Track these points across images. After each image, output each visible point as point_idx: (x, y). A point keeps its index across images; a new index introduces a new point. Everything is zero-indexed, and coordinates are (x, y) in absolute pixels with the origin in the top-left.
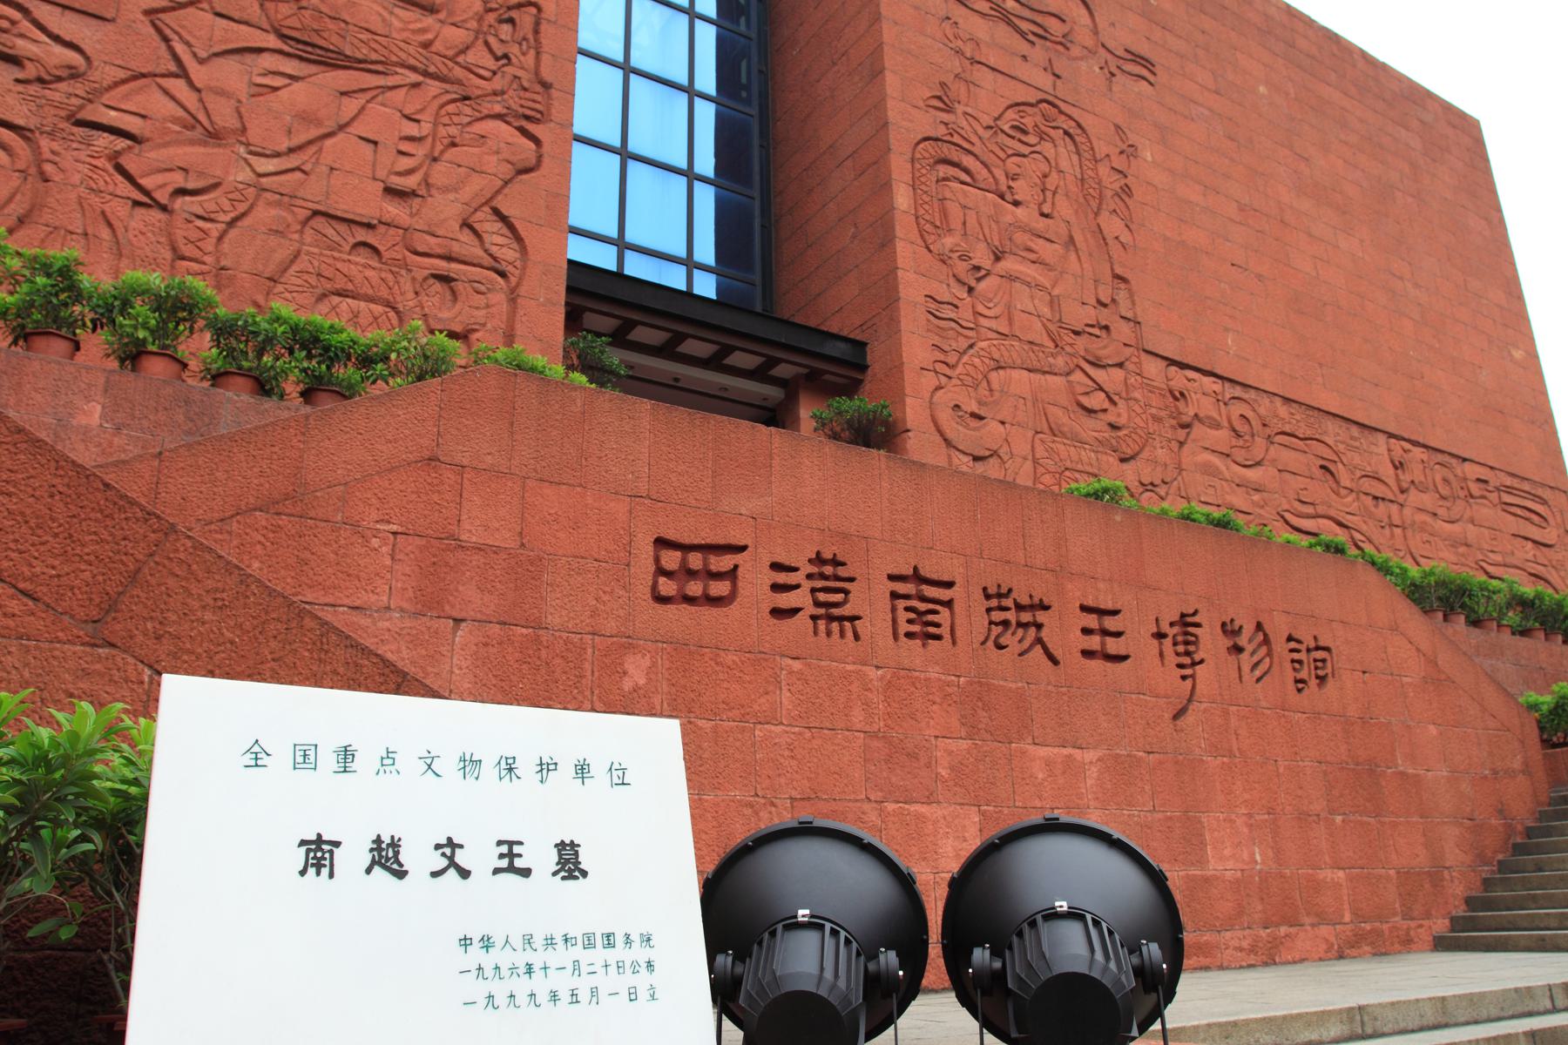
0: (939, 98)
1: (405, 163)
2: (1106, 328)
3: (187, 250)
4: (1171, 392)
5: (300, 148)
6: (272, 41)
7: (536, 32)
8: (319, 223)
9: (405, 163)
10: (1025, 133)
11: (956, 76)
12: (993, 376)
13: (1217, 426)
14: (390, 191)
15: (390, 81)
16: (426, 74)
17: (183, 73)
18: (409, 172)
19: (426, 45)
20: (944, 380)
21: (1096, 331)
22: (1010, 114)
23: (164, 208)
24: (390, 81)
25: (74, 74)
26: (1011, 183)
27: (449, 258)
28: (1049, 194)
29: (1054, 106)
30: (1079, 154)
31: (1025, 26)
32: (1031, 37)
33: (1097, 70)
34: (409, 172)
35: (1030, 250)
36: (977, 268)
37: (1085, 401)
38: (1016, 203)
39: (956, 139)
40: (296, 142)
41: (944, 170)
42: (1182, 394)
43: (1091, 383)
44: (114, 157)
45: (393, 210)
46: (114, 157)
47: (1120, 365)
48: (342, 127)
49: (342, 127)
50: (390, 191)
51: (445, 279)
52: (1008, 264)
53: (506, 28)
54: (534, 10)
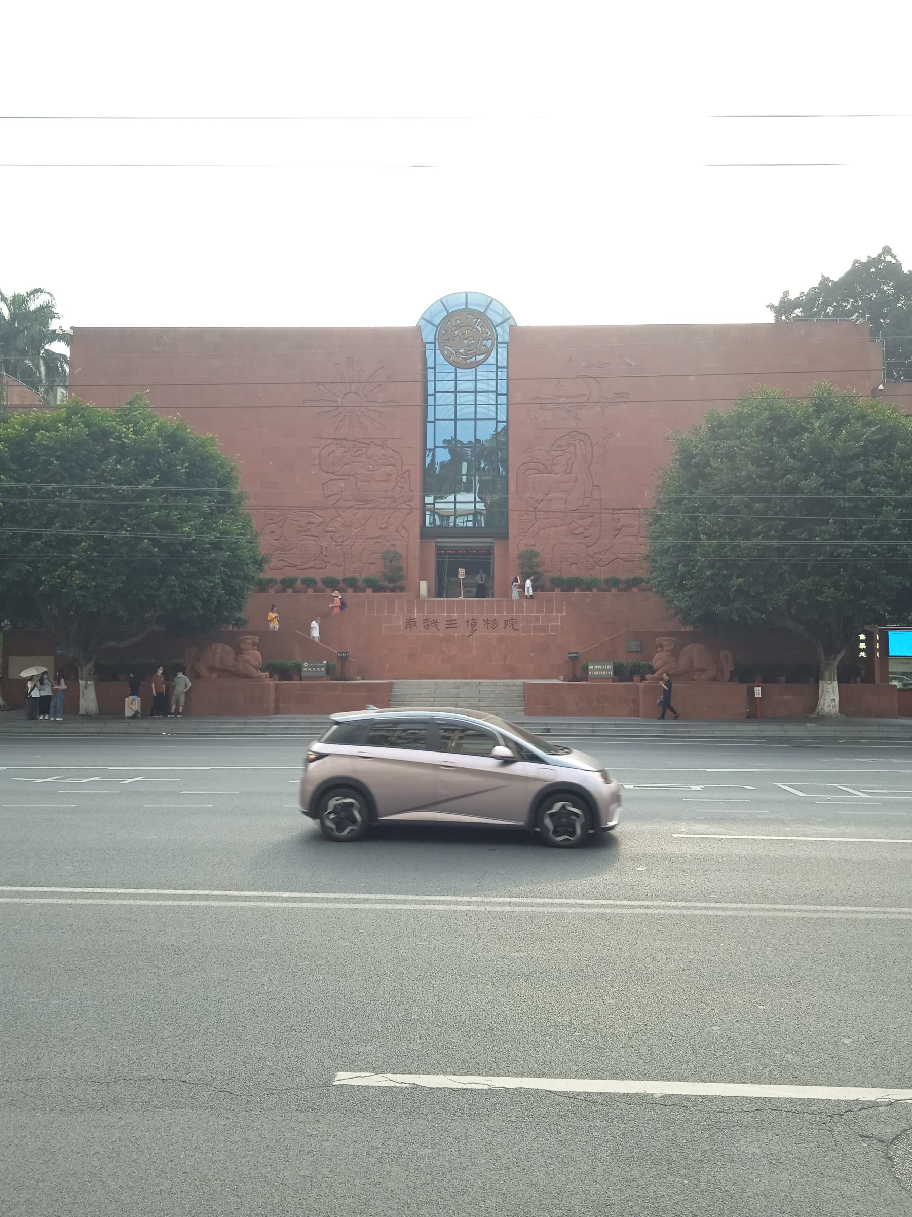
0: (529, 448)
1: (384, 521)
2: (588, 505)
3: (345, 552)
4: (614, 519)
5: (363, 525)
6: (355, 502)
7: (409, 477)
8: (368, 540)
9: (384, 521)
10: (563, 447)
11: (537, 437)
12: (541, 532)
13: (634, 526)
14: (381, 529)
15: (379, 503)
16: (385, 498)
17: (340, 516)
18: (384, 523)
19: (386, 491)
20: (522, 538)
21: (584, 507)
22: (557, 442)
23: (341, 545)
24: (379, 503)
25: (323, 522)
26: (554, 468)
27: (394, 540)
28: (570, 466)
29: (576, 431)
30: (585, 446)
31: (566, 406)
32: (569, 409)
33: (599, 409)
34: (384, 523)
35: (559, 488)
36: (538, 500)
37: (575, 532)
38: (556, 474)
39: (534, 460)
40: (362, 523)
41: (528, 473)
42: (618, 519)
43: (578, 526)
44: (332, 537)
45: (382, 533)
46: (332, 537)
47: (592, 516)
48: (370, 517)
49: (370, 517)
50: (381, 529)
51: (394, 545)
52: (551, 495)
53: (402, 479)
54: (408, 472)
